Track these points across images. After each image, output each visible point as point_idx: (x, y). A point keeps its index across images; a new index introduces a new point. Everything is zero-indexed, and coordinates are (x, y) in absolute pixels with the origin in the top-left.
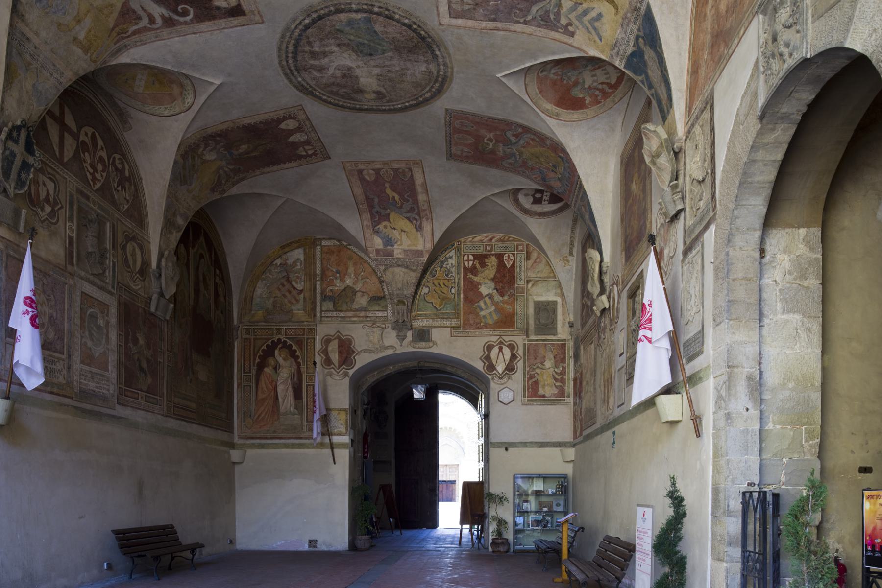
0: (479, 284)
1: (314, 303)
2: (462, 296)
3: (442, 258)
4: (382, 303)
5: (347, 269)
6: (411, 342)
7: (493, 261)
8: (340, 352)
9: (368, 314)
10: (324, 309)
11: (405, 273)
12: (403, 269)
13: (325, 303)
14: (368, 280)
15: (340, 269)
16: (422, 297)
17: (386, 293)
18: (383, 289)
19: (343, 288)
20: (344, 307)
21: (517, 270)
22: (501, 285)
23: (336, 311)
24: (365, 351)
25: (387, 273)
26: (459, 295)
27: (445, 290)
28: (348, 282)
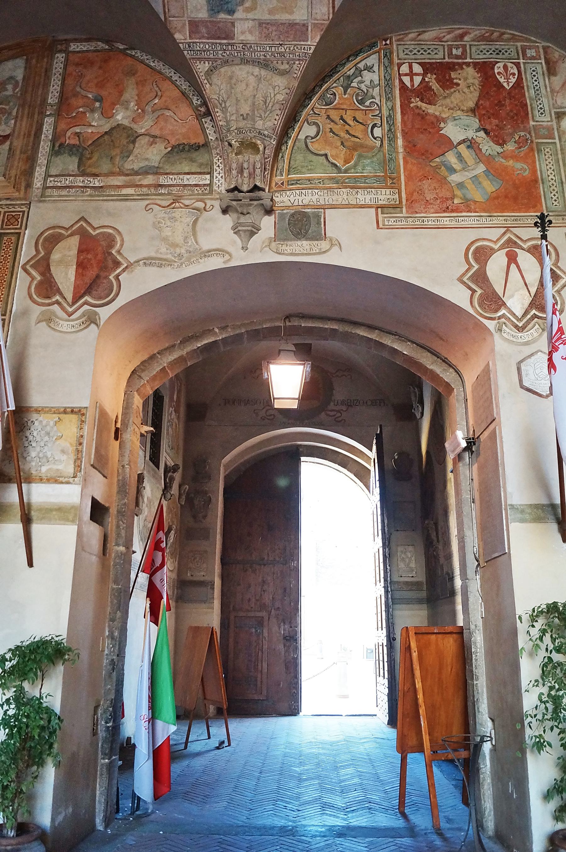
0: (439, 120)
2: (400, 142)
3: (348, 69)
4: (202, 157)
5: (121, 93)
6: (270, 240)
7: (468, 78)
8: (81, 266)
9: (163, 180)
10: (53, 172)
11: (259, 79)
12: (256, 70)
15: (104, 93)
18: (203, 130)
19: (106, 128)
21: (530, 93)
22: (495, 122)
23: (83, 174)
24: (148, 261)
25: (215, 79)
26: (392, 139)
27: (358, 130)
28: (121, 116)
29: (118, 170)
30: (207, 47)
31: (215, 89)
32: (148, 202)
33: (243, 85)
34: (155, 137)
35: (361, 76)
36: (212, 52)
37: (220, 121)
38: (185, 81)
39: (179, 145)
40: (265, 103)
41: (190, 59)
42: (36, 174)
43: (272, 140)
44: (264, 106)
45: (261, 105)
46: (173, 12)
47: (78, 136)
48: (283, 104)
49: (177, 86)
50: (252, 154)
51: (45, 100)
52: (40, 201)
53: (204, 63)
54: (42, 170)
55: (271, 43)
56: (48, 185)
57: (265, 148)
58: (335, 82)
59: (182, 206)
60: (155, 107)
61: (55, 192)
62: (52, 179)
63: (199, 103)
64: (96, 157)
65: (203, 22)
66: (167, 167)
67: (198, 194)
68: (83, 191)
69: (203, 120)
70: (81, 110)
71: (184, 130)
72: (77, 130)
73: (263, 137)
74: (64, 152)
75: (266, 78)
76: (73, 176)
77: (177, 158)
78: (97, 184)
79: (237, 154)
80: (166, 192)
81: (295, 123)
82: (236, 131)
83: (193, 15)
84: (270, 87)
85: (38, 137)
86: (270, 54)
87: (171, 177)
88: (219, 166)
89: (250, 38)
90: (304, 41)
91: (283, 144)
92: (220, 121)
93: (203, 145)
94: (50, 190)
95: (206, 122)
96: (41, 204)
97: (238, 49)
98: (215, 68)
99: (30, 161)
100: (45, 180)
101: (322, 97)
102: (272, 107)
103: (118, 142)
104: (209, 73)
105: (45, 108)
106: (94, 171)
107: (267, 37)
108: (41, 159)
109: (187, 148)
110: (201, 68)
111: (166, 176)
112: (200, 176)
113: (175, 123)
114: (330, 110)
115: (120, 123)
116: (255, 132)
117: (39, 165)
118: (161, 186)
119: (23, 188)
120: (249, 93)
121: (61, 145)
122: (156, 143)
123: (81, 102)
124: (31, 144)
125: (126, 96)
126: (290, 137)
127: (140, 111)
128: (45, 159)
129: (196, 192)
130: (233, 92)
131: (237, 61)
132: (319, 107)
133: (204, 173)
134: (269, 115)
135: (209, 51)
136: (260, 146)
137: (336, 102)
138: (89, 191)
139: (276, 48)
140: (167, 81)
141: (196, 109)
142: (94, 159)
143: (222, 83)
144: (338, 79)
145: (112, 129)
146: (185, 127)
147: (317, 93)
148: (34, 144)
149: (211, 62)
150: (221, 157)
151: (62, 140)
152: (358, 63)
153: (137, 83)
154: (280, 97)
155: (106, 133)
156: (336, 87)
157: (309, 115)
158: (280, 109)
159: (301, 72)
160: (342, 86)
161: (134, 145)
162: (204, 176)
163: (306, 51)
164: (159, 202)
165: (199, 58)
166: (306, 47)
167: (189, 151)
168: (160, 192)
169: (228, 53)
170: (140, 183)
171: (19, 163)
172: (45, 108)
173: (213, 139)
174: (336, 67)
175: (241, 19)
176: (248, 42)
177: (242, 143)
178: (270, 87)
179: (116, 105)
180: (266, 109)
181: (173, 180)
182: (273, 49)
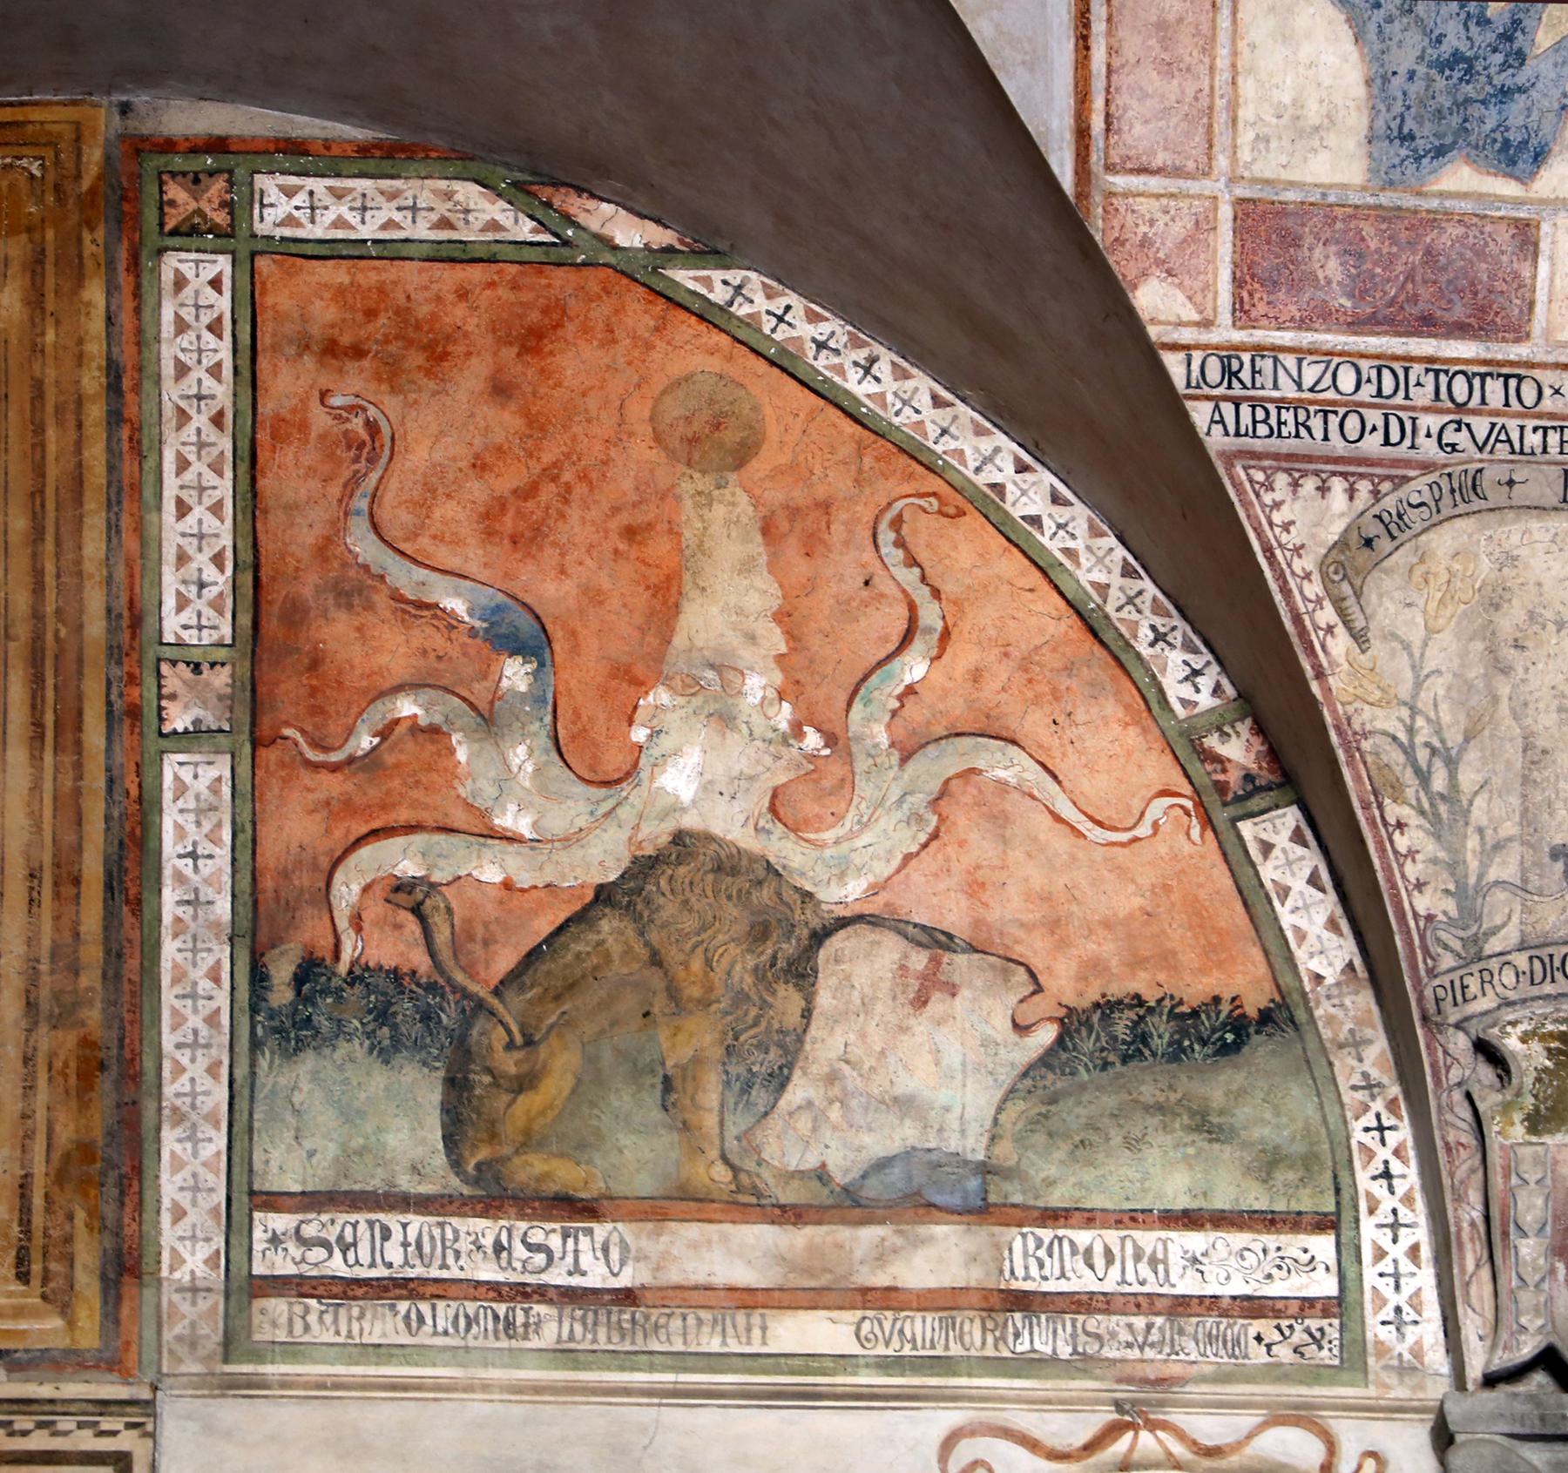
1: (111, 1072)
4: (1262, 1100)
5: (665, 598)
9: (1031, 1259)
13: (301, 1080)
14: (1006, 766)
18: (1255, 901)
19: (602, 858)
20: (636, 1153)
23: (494, 1195)
28: (694, 776)
29: (721, 1173)
32: (948, 1418)
34: (937, 940)
38: (1095, 533)
39: (1107, 1008)
42: (169, 1186)
47: (417, 910)
51: (136, 622)
52: (231, 1386)
54: (207, 1151)
56: (258, 1269)
59: (1178, 1449)
60: (912, 710)
61: (321, 1324)
62: (281, 1222)
63: (1205, 700)
64: (562, 1066)
66: (1052, 1171)
67: (1275, 1372)
68: (509, 1324)
69: (1246, 828)
70: (407, 707)
71: (1127, 901)
72: (404, 859)
74: (340, 1030)
76: (423, 1204)
77: (1110, 1101)
78: (596, 1276)
79: (1535, 1124)
80: (1065, 1351)
82: (1521, 960)
85: (137, 905)
87: (1083, 1237)
88: (1387, 1175)
93: (1266, 1017)
94: (278, 1306)
95: (1267, 848)
96: (231, 1411)
99: (105, 1084)
100: (235, 1225)
103: (697, 964)
105: (150, 681)
106: (566, 1175)
108: (179, 1070)
109: (1161, 1032)
111: (1046, 1234)
112: (1271, 1240)
113: (1060, 843)
115: (690, 821)
117: (179, 1117)
118: (1022, 1302)
119: (87, 1283)
121: (309, 971)
122: (952, 990)
123: (395, 650)
124: (92, 953)
125: (704, 622)
127: (813, 740)
128: (212, 1071)
129: (1258, 1355)
133: (1294, 1222)
138: (551, 1326)
140: (973, 520)
141: (1188, 746)
142: (555, 1086)
145: (644, 868)
148: (114, 955)
150: (1392, 1106)
151: (311, 932)
153: (767, 530)
155: (604, 895)
161: (809, 999)
162: (1294, 1244)
164: (1023, 1420)
167: (1177, 1053)
168: (1023, 1346)
170: (881, 1280)
171: (29, 1089)
172: (150, 681)
179: (640, 685)
181: (1099, 1262)
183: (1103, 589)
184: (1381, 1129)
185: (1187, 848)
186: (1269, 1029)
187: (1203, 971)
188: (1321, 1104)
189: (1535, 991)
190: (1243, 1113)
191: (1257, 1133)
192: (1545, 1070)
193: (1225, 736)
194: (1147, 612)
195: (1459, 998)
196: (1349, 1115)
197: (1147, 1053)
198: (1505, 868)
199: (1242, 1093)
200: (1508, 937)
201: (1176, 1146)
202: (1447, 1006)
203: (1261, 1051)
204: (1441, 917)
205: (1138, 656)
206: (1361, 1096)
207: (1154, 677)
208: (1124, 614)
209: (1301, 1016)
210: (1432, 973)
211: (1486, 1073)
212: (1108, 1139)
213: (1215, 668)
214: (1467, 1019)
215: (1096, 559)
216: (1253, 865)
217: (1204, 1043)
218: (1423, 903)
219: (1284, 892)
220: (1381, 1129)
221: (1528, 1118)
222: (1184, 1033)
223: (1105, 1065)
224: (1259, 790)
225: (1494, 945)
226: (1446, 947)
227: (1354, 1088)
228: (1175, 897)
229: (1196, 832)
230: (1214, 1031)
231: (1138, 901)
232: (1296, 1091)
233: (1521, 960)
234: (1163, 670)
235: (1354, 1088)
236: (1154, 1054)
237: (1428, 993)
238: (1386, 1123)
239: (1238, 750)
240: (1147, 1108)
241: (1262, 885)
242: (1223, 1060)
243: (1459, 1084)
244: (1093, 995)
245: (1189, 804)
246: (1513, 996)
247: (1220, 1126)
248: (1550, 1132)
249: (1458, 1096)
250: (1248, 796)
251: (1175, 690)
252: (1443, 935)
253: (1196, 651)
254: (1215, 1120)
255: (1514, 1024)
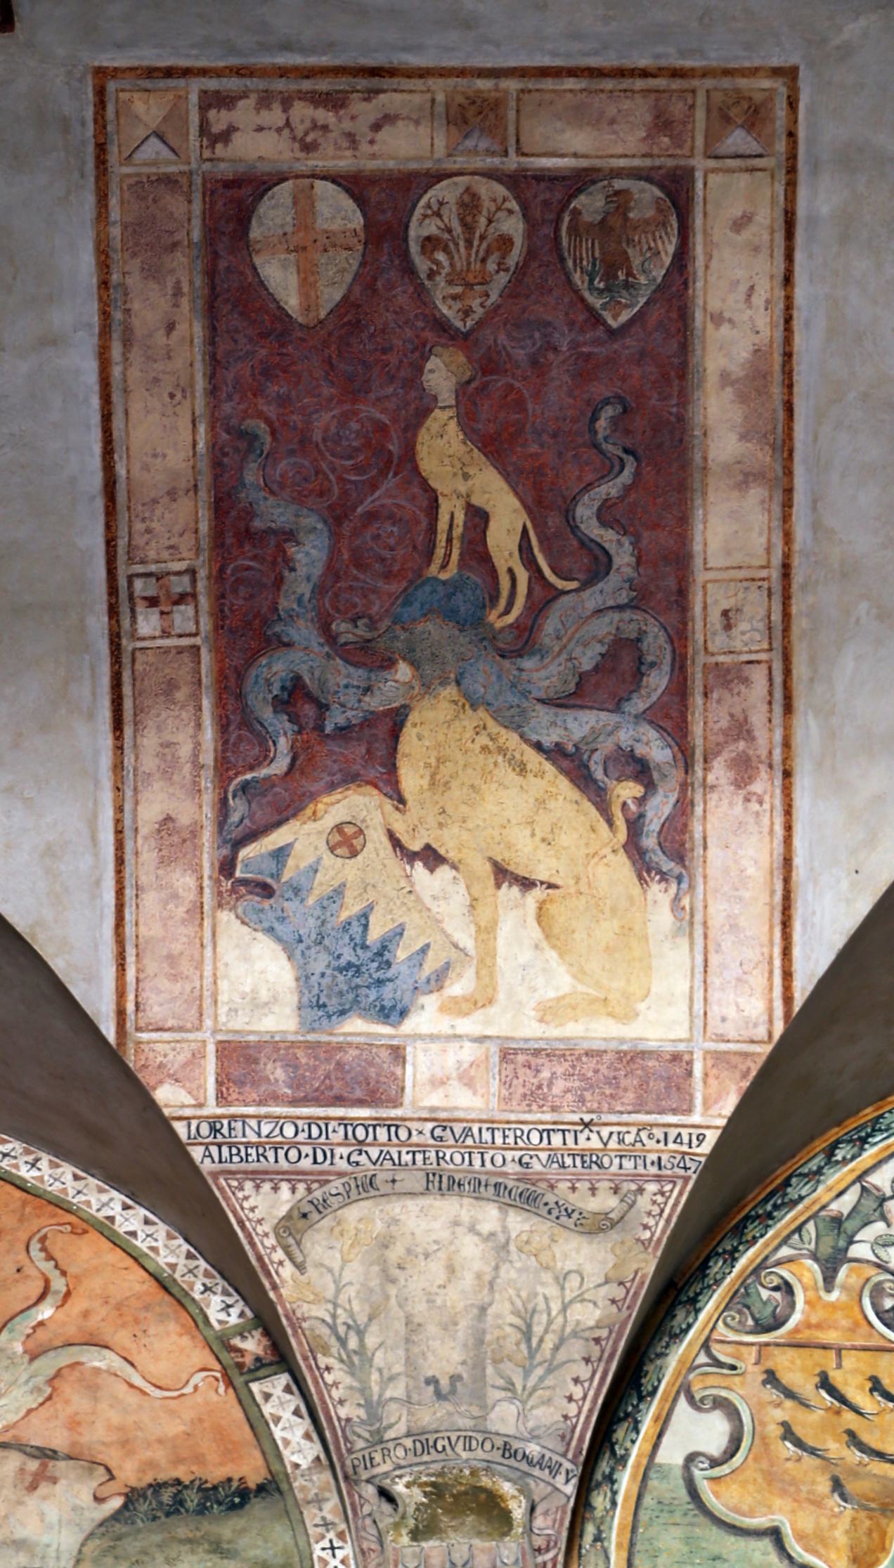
11: (501, 1247)
16: (670, 1488)
17: (297, 1445)
18: (258, 1426)
25: (317, 1246)
30: (289, 1131)
31: (318, 1282)
33: (436, 1270)
35: (884, 1218)
36: (306, 1150)
37: (341, 1402)
40: (527, 1334)
41: (215, 1175)
43: (561, 1478)
44: (523, 1346)
45: (510, 1345)
46: (156, 1010)
48: (597, 1341)
49: (137, 1258)
50: (479, 1534)
53: (276, 1189)
55: (548, 1117)
57: (532, 1509)
58: (785, 1241)
63: (234, 1319)
65: (275, 1047)
69: (255, 1387)
73: (524, 1466)
75: (527, 1242)
79: (416, 1535)
81: (641, 1398)
82: (408, 1443)
83: (238, 1023)
84: (547, 1277)
86: (544, 1156)
89: (465, 1101)
90: (675, 1111)
91: (599, 1485)
92: (341, 1402)
93: (261, 1489)
95: (267, 1397)
97: (415, 1139)
98: (321, 1207)
101: (740, 1299)
102: (556, 1348)
104: (294, 1226)
107: (535, 1096)
109: (192, 1499)
110: (260, 1209)
114: (776, 1351)
116: (488, 1446)
120: (458, 1296)
126: (623, 1460)
130: (392, 1291)
131: (414, 1181)
132: (733, 1337)
134: (541, 1379)
135: (295, 1145)
136: (512, 1505)
137: (796, 1318)
139: (570, 1138)
141: (221, 1344)
143: (345, 1262)
144: (799, 1229)
146: (173, 1413)
147: (718, 1282)
149: (301, 1187)
150: (341, 1536)
152: (866, 1172)
154: (587, 1315)
156: (790, 1260)
157: (692, 1369)
158: (587, 1360)
159: (668, 1221)
160: (814, 1256)
163: (685, 1148)
165: (253, 1172)
166: (685, 1132)
167: (202, 1510)
169: (374, 1152)
173: (305, 1464)
174: (786, 1183)
175: (433, 1038)
176: (461, 1115)
177: (436, 1491)
178: (547, 1277)
180: (532, 1355)
182: (557, 1140)
183: (173, 1267)
184: (333, 1548)
185: (215, 1398)
186: (263, 1495)
187: (221, 1464)
188: (295, 1536)
189: (417, 1460)
190: (243, 1542)
191: (252, 1553)
192: (422, 1504)
193: (244, 1338)
194: (201, 1276)
195: (368, 1465)
196: (312, 1541)
197: (182, 1510)
198: (397, 1390)
199: (243, 1531)
200: (401, 1428)
201: (200, 1561)
202: (361, 1469)
203: (257, 1507)
204: (355, 1419)
205: (193, 1299)
206: (320, 1530)
207: (201, 1310)
208: (186, 1278)
209: (284, 1486)
210: (350, 1451)
211: (386, 1507)
212: (154, 1559)
213: (241, 1303)
214: (374, 1477)
215: (167, 1248)
216: (258, 1406)
217: (220, 1504)
218: (343, 1412)
219: (277, 1420)
220: (333, 1548)
221: (411, 1532)
222: (207, 1498)
223: (155, 1518)
224: (263, 1366)
225: (390, 1434)
226: (359, 1436)
227: (316, 1526)
228: (206, 1425)
229: (222, 1389)
230: (227, 1496)
231: (182, 1428)
232: (278, 1528)
233: (408, 1443)
234: (208, 1305)
235: (316, 1526)
236: (187, 1511)
237: (348, 1463)
238: (336, 1545)
239: (253, 1345)
240: (182, 1542)
241: (263, 1416)
242: (232, 1513)
243: (370, 1515)
244: (149, 1479)
245: (218, 1375)
246: (403, 1463)
247: (228, 1550)
248: (426, 1540)
249: (368, 1521)
250: (257, 1369)
251: (214, 1314)
252: (358, 1430)
253: (229, 1295)
254: (225, 1546)
255: (400, 1477)
